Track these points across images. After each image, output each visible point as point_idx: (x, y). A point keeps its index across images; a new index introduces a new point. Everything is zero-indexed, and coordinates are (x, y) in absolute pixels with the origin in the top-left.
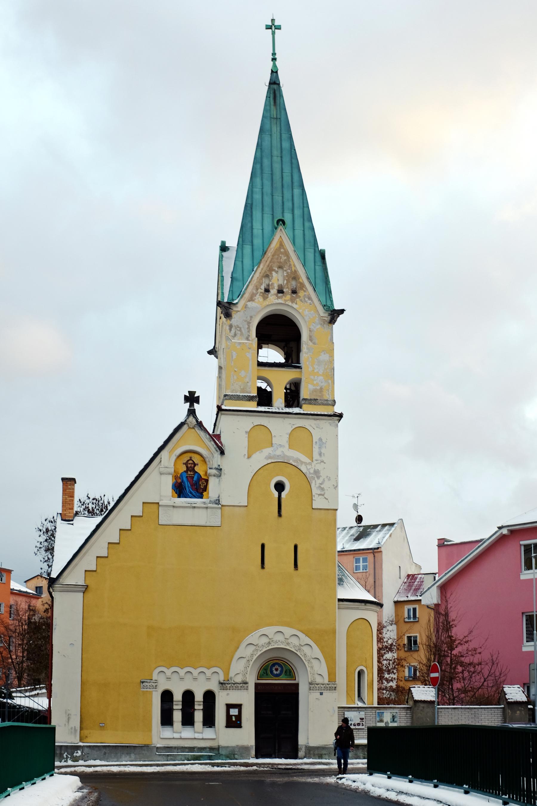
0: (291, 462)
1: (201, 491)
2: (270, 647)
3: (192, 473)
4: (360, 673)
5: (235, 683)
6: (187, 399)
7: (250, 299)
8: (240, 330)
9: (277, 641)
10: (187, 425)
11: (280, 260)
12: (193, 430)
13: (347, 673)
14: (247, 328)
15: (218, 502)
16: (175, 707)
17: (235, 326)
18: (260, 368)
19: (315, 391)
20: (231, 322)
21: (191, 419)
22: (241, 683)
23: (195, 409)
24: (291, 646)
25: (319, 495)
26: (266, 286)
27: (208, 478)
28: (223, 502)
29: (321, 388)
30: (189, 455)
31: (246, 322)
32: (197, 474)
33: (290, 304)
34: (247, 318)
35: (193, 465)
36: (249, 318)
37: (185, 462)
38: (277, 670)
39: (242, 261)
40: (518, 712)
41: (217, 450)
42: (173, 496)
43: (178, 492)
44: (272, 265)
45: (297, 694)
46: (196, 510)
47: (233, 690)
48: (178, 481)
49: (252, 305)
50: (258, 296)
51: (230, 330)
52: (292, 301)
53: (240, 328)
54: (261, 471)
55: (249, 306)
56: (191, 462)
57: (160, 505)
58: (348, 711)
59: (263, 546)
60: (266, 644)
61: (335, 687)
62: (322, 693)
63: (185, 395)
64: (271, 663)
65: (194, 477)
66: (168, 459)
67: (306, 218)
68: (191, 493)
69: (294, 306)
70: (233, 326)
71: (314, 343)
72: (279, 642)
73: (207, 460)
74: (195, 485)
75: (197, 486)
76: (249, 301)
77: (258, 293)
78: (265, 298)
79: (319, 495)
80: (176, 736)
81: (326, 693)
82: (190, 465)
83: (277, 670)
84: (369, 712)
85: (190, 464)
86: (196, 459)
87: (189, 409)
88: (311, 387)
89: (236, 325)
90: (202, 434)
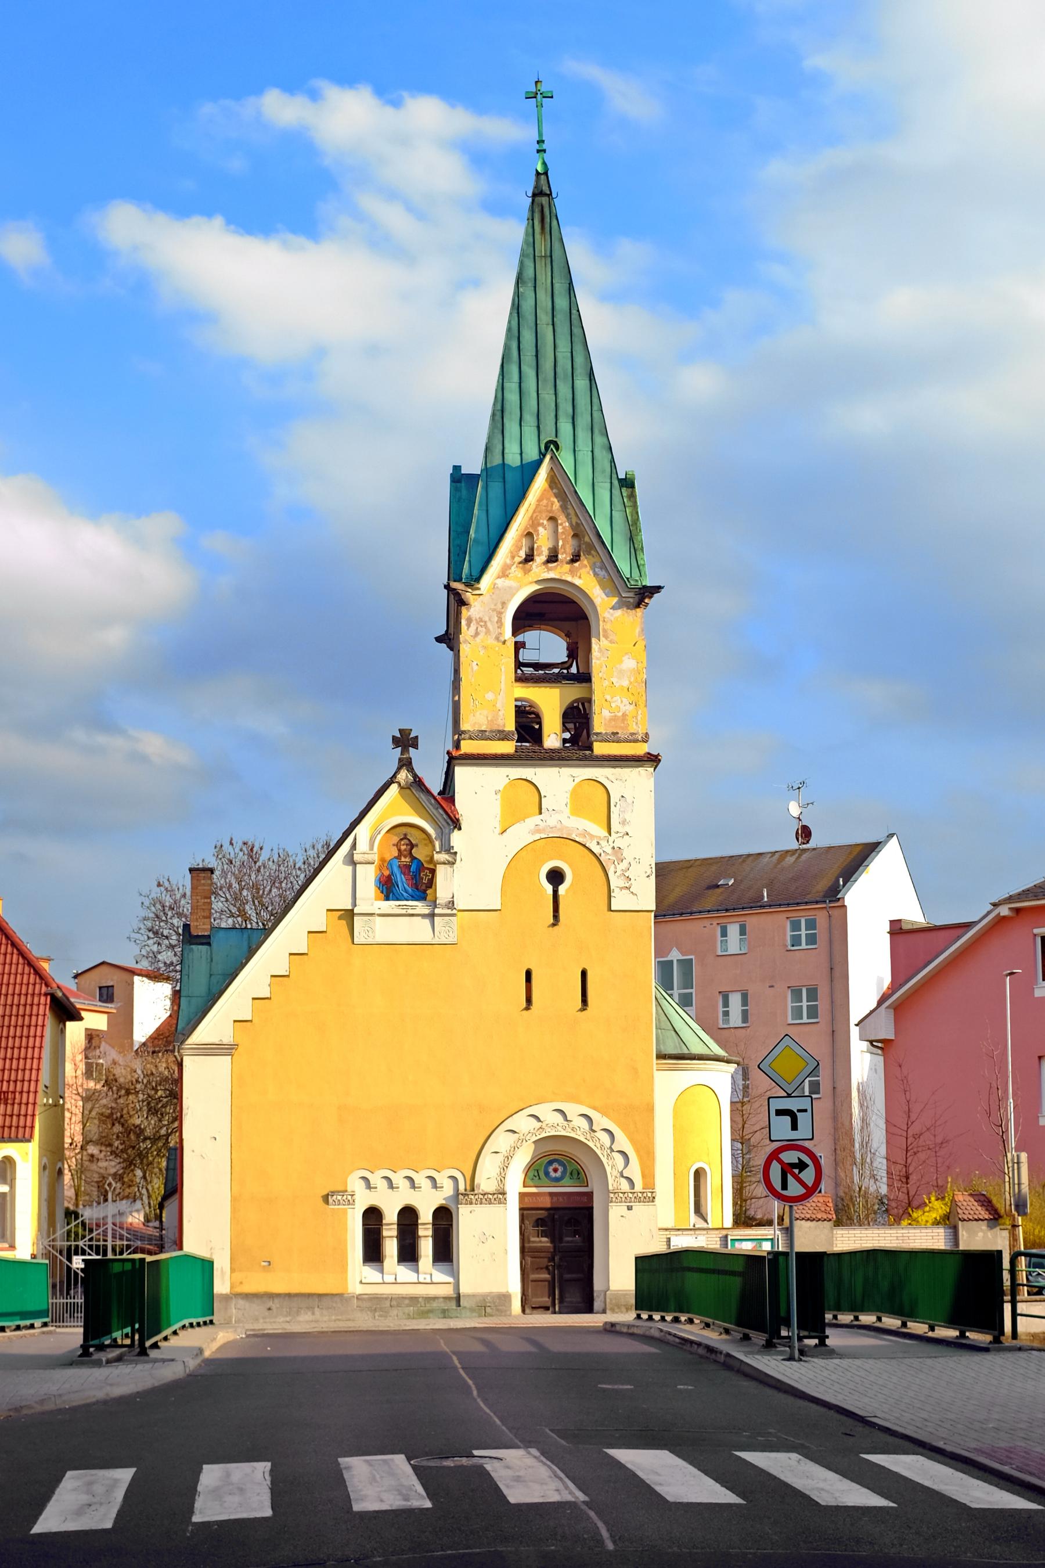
0: (573, 837)
1: (424, 887)
2: (544, 1135)
4: (699, 1174)
5: (485, 1194)
6: (396, 742)
7: (501, 574)
8: (486, 626)
9: (556, 1125)
11: (552, 507)
13: (675, 1174)
14: (497, 622)
15: (451, 904)
16: (385, 1233)
17: (476, 620)
18: (518, 684)
19: (614, 719)
20: (469, 613)
21: (403, 776)
22: (494, 1194)
23: (411, 759)
24: (579, 1132)
25: (621, 888)
26: (527, 551)
27: (436, 867)
28: (460, 904)
29: (624, 715)
30: (404, 830)
31: (495, 613)
33: (569, 579)
34: (495, 605)
35: (409, 847)
36: (499, 606)
38: (556, 1170)
39: (487, 511)
40: (981, 1234)
42: (377, 899)
44: (537, 516)
45: (590, 1210)
47: (481, 1204)
49: (505, 584)
50: (513, 568)
51: (469, 625)
52: (572, 572)
53: (485, 622)
54: (524, 853)
55: (499, 586)
57: (356, 914)
58: (676, 1235)
59: (529, 974)
60: (536, 1129)
61: (654, 1198)
62: (632, 1206)
63: (393, 736)
64: (546, 1160)
67: (596, 431)
68: (406, 892)
69: (577, 582)
70: (473, 619)
71: (611, 642)
72: (558, 1127)
76: (499, 577)
77: (514, 563)
78: (527, 572)
79: (621, 888)
80: (389, 1278)
81: (638, 1207)
82: (405, 847)
83: (556, 1170)
84: (714, 1236)
86: (414, 836)
87: (400, 759)
88: (606, 713)
89: (478, 617)
90: (423, 797)
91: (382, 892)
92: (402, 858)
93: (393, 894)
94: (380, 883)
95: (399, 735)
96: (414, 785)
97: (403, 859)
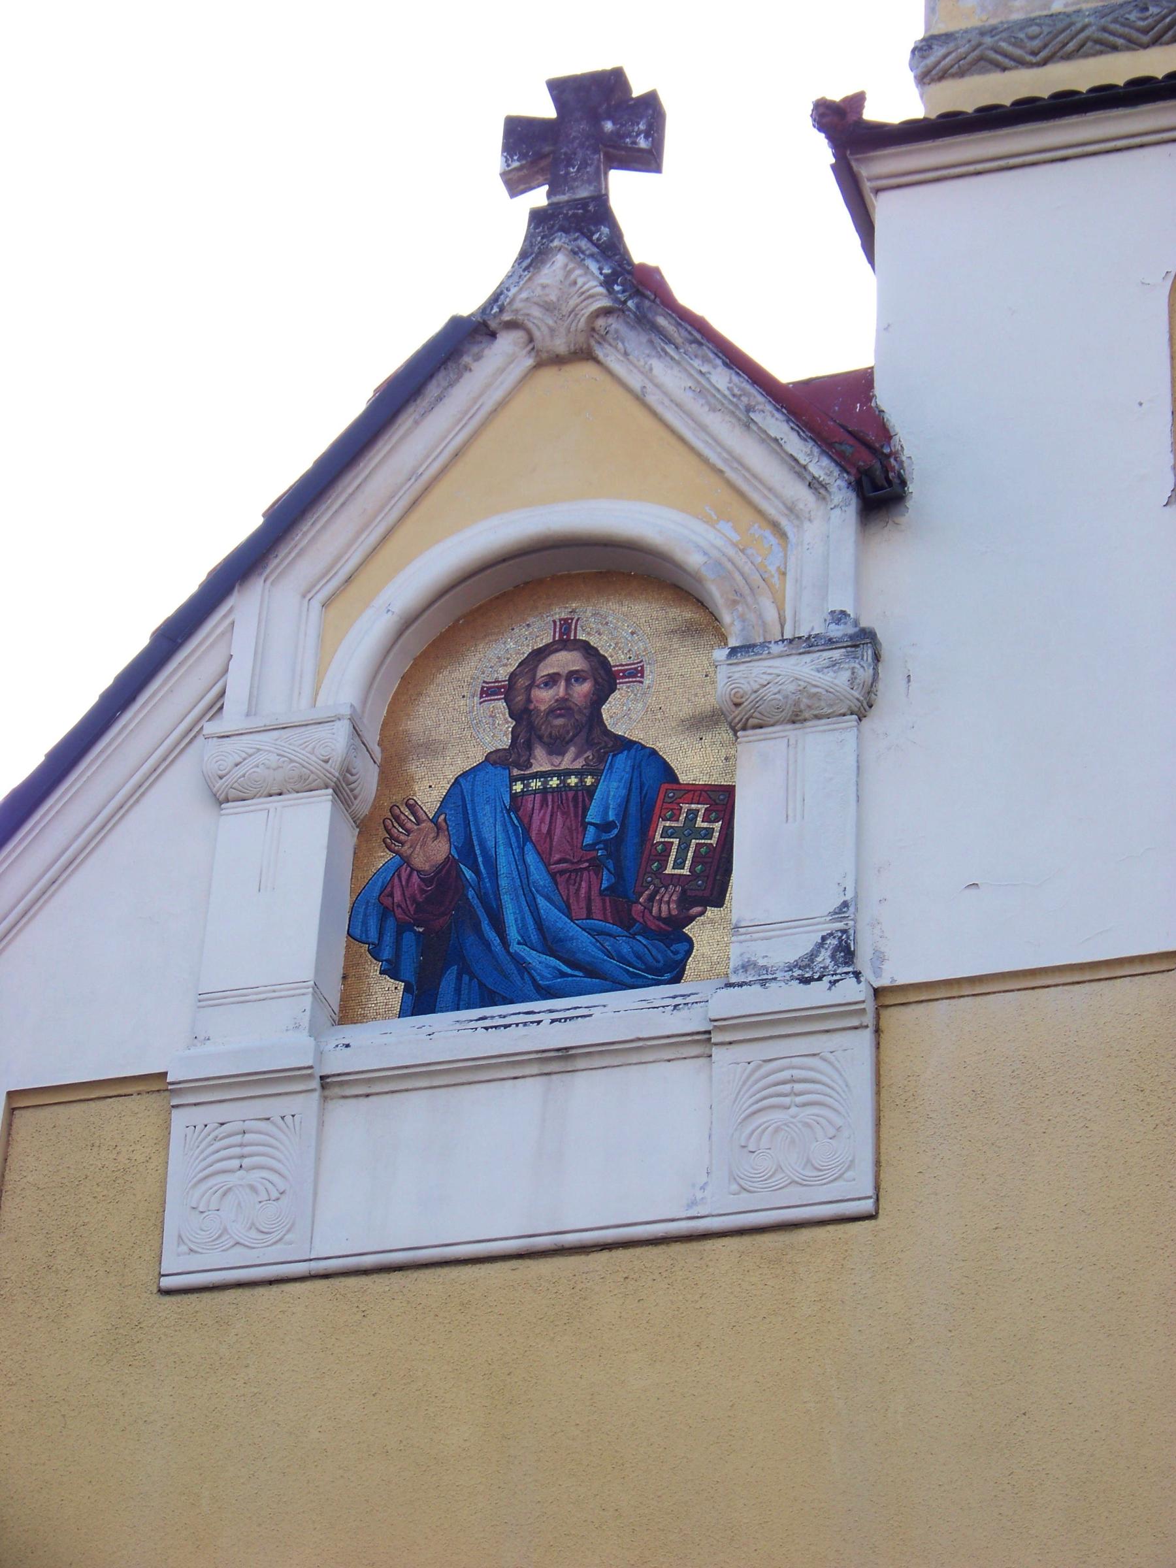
1: (667, 905)
3: (567, 761)
10: (517, 336)
12: (585, 371)
32: (622, 762)
35: (585, 687)
37: (503, 674)
41: (816, 486)
43: (408, 966)
46: (554, 1077)
48: (419, 861)
56: (565, 661)
65: (591, 791)
66: (309, 665)
68: (550, 943)
73: (716, 594)
74: (596, 866)
75: (619, 874)
85: (552, 680)
91: (391, 971)
92: (539, 752)
93: (465, 969)
94: (385, 912)
95: (546, 110)
96: (614, 324)
97: (541, 761)
